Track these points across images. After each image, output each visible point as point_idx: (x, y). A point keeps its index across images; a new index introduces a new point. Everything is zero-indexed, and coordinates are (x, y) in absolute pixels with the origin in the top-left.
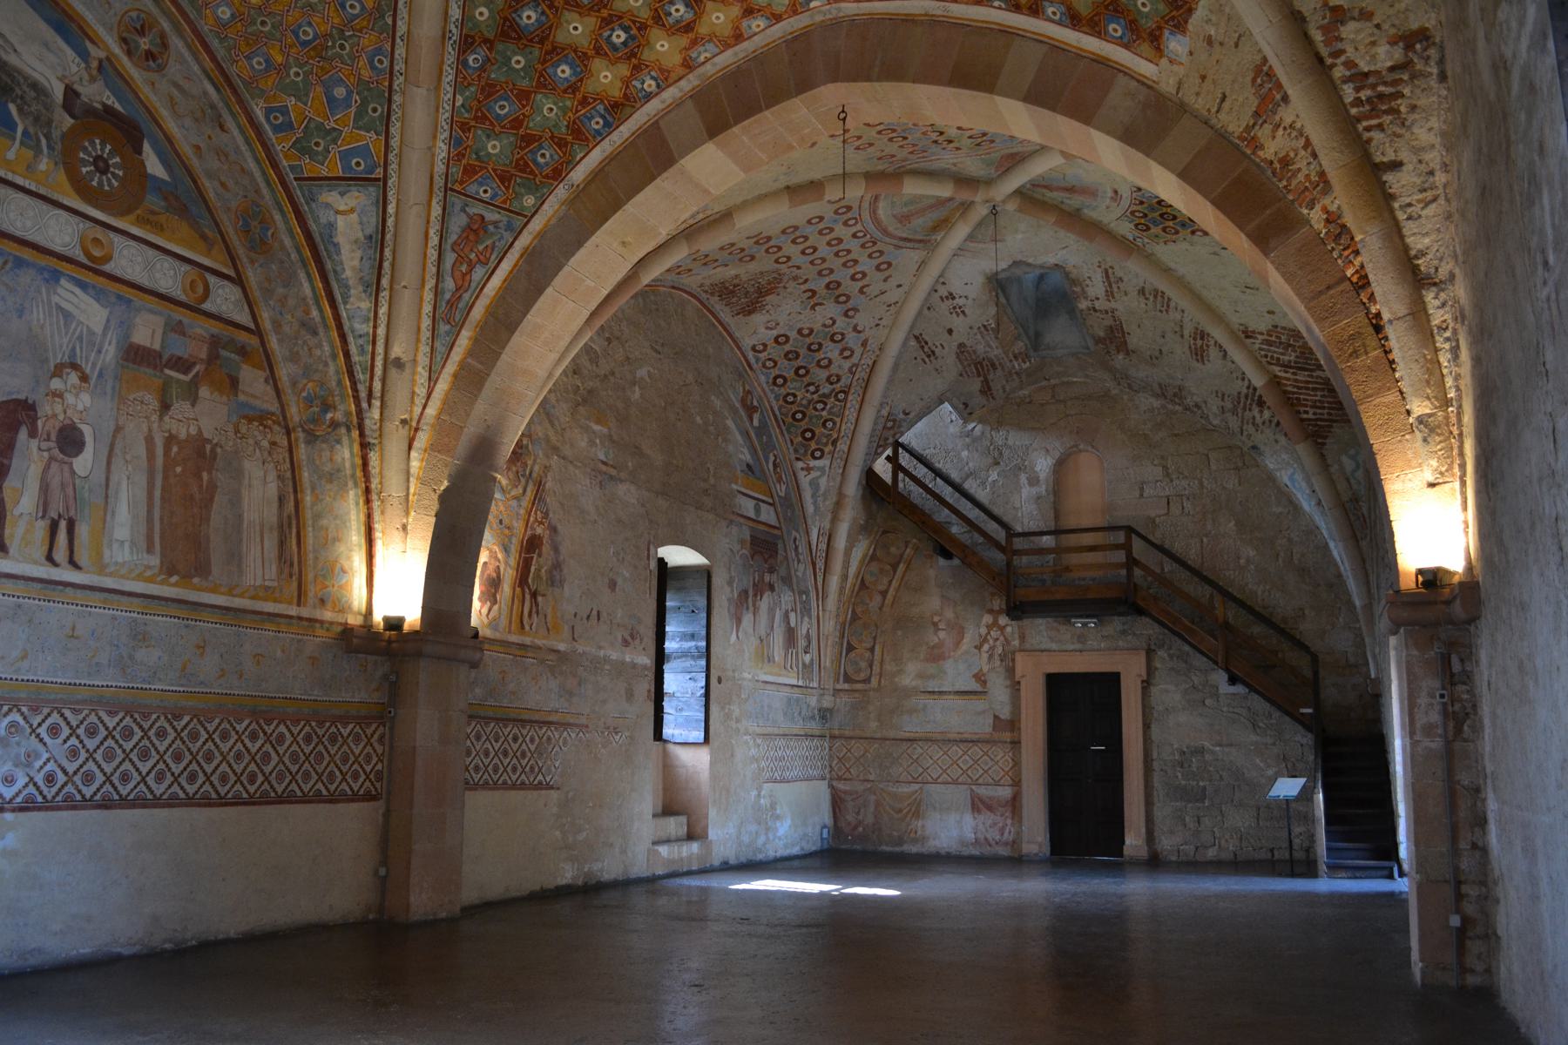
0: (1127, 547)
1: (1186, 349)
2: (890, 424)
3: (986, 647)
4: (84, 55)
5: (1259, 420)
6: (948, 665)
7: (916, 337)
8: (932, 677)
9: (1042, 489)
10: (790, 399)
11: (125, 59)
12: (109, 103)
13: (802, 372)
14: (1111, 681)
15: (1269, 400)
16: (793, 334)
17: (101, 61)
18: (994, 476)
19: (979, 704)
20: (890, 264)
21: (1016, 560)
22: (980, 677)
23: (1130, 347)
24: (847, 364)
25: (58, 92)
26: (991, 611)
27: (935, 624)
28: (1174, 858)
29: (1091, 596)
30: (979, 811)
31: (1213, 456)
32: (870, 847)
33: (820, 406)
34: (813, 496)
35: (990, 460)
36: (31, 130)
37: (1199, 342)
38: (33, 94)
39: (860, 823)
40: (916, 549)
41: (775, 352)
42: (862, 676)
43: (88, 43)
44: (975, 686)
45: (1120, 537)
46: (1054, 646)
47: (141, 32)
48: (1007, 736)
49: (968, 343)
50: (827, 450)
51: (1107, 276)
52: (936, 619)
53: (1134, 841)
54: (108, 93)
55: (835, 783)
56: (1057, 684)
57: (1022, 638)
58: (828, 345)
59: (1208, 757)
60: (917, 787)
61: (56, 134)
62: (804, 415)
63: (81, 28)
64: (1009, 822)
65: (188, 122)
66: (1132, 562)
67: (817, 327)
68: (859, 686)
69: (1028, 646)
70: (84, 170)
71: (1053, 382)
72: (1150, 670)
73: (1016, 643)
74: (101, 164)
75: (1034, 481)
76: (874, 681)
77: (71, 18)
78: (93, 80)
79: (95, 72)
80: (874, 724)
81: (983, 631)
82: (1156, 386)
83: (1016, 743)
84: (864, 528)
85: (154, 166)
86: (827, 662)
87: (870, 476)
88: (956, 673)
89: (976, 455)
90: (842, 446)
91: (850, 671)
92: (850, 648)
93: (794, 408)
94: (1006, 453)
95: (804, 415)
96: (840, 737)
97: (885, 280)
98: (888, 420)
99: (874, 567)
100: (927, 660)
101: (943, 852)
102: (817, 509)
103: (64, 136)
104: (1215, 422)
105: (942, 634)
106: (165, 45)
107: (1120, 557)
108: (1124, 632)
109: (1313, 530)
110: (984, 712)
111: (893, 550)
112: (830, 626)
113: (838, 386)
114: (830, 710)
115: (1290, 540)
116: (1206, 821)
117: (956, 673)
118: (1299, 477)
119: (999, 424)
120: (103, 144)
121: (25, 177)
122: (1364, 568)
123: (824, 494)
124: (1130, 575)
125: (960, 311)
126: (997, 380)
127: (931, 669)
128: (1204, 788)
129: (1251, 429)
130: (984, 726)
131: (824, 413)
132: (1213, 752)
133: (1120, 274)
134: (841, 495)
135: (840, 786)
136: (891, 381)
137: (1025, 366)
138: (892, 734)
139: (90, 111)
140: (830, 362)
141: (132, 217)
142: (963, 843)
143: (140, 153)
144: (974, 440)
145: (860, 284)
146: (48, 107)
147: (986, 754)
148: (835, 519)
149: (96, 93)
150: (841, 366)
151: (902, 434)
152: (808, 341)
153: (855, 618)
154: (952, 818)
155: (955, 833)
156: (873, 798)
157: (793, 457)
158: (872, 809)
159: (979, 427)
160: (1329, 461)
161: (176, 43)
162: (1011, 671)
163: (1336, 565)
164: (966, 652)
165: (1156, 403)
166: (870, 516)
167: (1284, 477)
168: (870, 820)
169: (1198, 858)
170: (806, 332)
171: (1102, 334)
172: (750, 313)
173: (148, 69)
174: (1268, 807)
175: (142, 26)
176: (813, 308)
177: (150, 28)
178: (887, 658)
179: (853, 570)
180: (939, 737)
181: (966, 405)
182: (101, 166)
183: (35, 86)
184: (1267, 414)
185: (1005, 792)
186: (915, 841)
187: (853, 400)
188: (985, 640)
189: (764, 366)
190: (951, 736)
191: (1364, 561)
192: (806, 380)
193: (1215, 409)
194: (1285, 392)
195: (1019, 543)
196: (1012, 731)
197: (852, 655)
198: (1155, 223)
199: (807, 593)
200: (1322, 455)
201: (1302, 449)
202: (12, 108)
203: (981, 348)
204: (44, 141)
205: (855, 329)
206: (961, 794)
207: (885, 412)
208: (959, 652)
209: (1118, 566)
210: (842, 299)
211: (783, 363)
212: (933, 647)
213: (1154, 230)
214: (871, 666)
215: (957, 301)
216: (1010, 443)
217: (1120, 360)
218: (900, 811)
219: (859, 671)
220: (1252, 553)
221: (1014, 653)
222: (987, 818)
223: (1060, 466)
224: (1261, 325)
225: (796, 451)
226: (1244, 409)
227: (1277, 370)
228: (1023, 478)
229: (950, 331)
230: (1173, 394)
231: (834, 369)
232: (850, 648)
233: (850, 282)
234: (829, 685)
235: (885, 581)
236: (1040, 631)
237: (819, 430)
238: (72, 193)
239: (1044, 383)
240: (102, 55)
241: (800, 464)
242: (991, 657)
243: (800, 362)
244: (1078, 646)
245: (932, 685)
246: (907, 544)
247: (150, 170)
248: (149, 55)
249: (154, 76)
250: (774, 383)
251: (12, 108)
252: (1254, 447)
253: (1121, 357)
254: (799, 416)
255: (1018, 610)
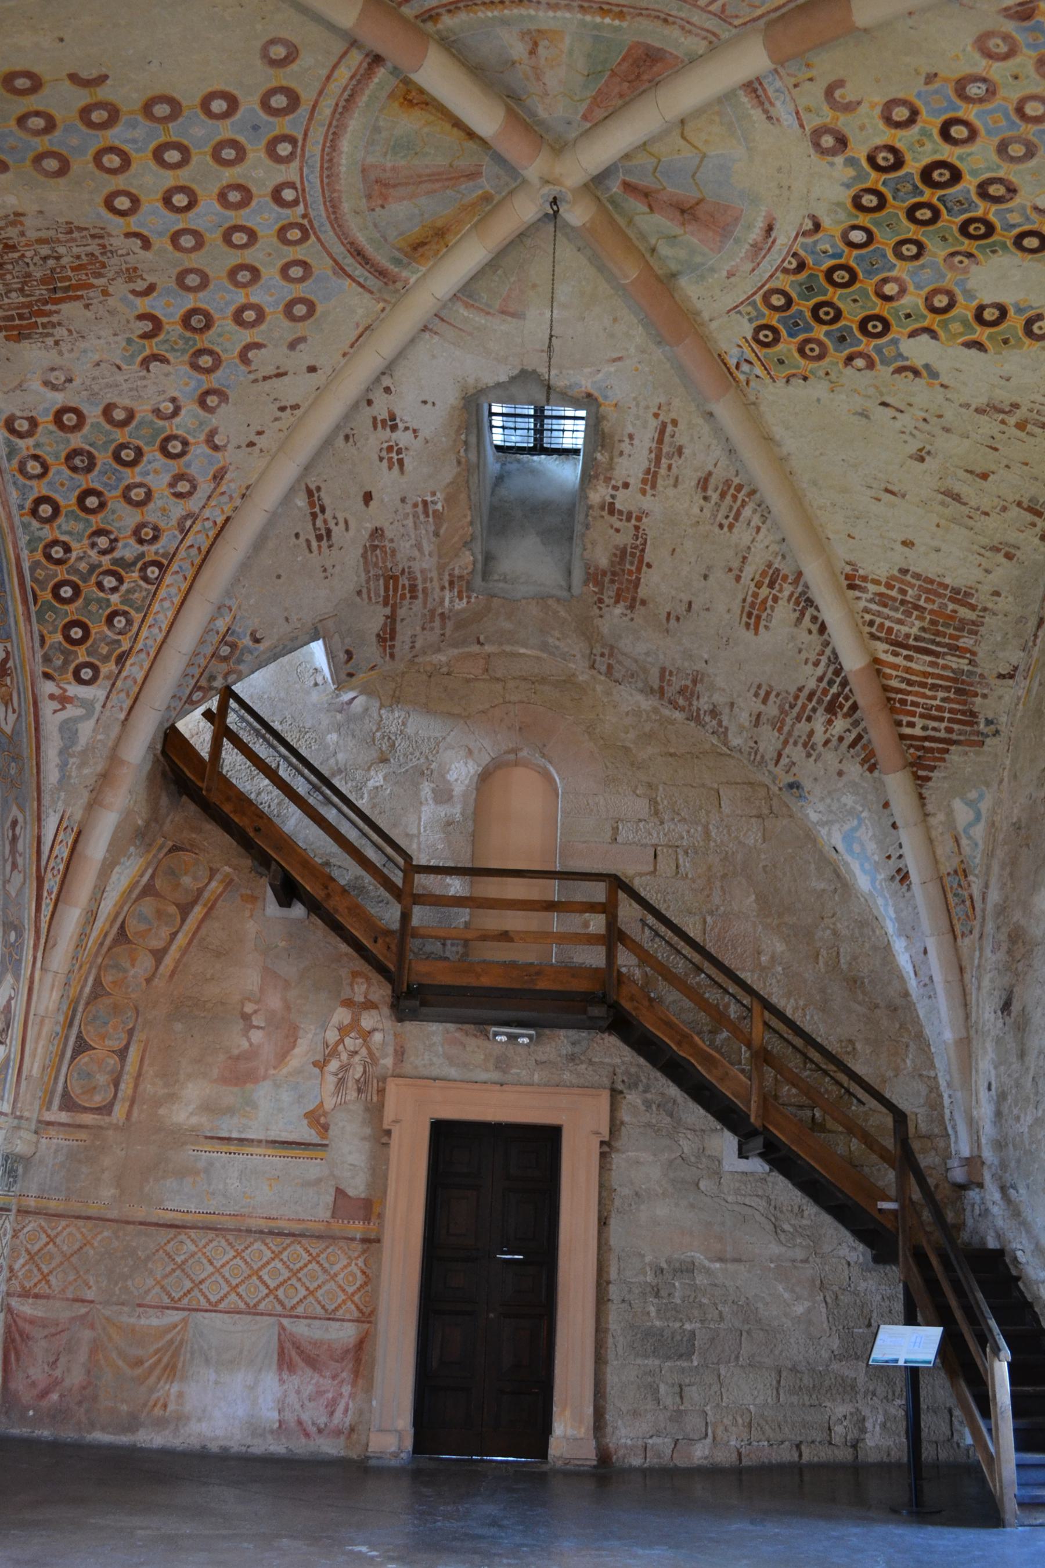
0: (609, 909)
1: (736, 609)
2: (225, 650)
3: (334, 1065)
5: (819, 738)
6: (263, 1093)
7: (310, 493)
8: (230, 1111)
9: (456, 811)
10: (57, 552)
13: (92, 502)
14: (546, 1140)
15: (865, 694)
16: (93, 413)
18: (377, 778)
19: (312, 1168)
20: (311, 307)
21: (419, 915)
22: (317, 1119)
23: (642, 592)
24: (178, 510)
26: (348, 1003)
27: (246, 1017)
28: (636, 1462)
29: (542, 985)
30: (291, 1368)
31: (726, 793)
32: (68, 1434)
33: (109, 582)
34: (64, 752)
35: (374, 754)
37: (764, 591)
39: (56, 1383)
40: (228, 883)
41: (51, 443)
42: (98, 1100)
44: (310, 1135)
45: (598, 892)
46: (453, 1072)
48: (357, 1228)
49: (388, 534)
50: (106, 669)
51: (660, 441)
52: (249, 1008)
53: (569, 1433)
55: (14, 1302)
56: (446, 1136)
57: (400, 1054)
58: (153, 456)
59: (700, 1279)
60: (176, 1316)
62: (77, 590)
64: (346, 1389)
66: (614, 937)
67: (143, 410)
68: (88, 1118)
69: (407, 1068)
71: (488, 648)
72: (615, 1126)
73: (388, 1062)
75: (443, 795)
76: (119, 1111)
80: (108, 1193)
81: (332, 1036)
82: (655, 672)
83: (371, 1242)
84: (139, 835)
86: (34, 1067)
87: (172, 740)
88: (276, 1109)
89: (351, 743)
90: (134, 669)
91: (75, 1090)
92: (82, 1047)
93: (61, 573)
94: (401, 745)
95: (77, 590)
96: (37, 1213)
97: (292, 346)
98: (223, 641)
99: (148, 906)
100: (224, 1080)
101: (214, 1447)
102: (64, 778)
104: (735, 741)
105: (256, 1036)
107: (597, 924)
108: (572, 1058)
109: (868, 923)
110: (318, 1181)
111: (186, 880)
112: (49, 1000)
113: (151, 551)
114: (26, 1160)
115: (835, 933)
116: (693, 1393)
117: (276, 1109)
118: (866, 835)
119: (396, 699)
122: (962, 980)
123: (84, 752)
124: (611, 957)
125: (394, 458)
126: (411, 612)
127: (229, 1095)
128: (693, 1333)
129: (796, 753)
130: (316, 1208)
131: (115, 598)
132: (708, 1272)
133: (682, 439)
134: (114, 759)
135: (26, 1308)
136: (245, 567)
137: (460, 605)
138: (141, 1213)
140: (149, 495)
142: (255, 1429)
144: (351, 719)
145: (247, 336)
147: (314, 1259)
148: (94, 804)
150: (164, 511)
151: (240, 679)
152: (119, 436)
153: (98, 991)
154: (238, 1381)
155: (241, 1411)
156: (87, 1334)
157: (40, 669)
158: (82, 1356)
159: (361, 700)
160: (930, 808)
162: (375, 1111)
163: (901, 979)
164: (299, 1072)
165: (646, 703)
166: (155, 817)
167: (834, 837)
168: (76, 1378)
169: (681, 1462)
170: (119, 415)
171: (604, 562)
172: (20, 337)
174: (794, 1370)
176: (146, 363)
178: (149, 1071)
179: (107, 906)
180: (231, 1224)
181: (349, 654)
184: (840, 724)
185: (345, 1333)
186: (161, 1423)
187: (173, 584)
188: (334, 1053)
189: (22, 470)
190: (254, 1223)
191: (961, 969)
192: (96, 521)
193: (744, 718)
194: (886, 689)
195: (425, 883)
196: (367, 1219)
197: (84, 1059)
198: (794, 329)
199: (19, 930)
200: (921, 797)
201: (897, 784)
203: (405, 547)
205: (210, 440)
206: (262, 1334)
207: (221, 625)
208: (285, 1071)
209: (592, 939)
210: (206, 361)
211: (59, 471)
212: (238, 1058)
213: (787, 346)
214: (116, 1084)
215: (402, 438)
216: (410, 731)
217: (614, 617)
218: (139, 1362)
219: (93, 1090)
220: (780, 947)
221: (383, 1079)
222: (305, 1381)
223: (485, 777)
224: (879, 566)
225: (47, 659)
226: (798, 719)
227: (881, 649)
228: (426, 789)
229: (368, 497)
230: (678, 692)
231: (151, 514)
232: (82, 1047)
233: (230, 325)
234: (31, 1111)
235: (165, 932)
236: (433, 1042)
237: (98, 628)
239: (475, 648)
241: (49, 687)
242: (341, 1082)
243: (93, 480)
244: (495, 1076)
245: (228, 1127)
246: (213, 872)
250: (34, 512)
252: (794, 786)
253: (618, 610)
254: (66, 592)
255: (411, 1000)
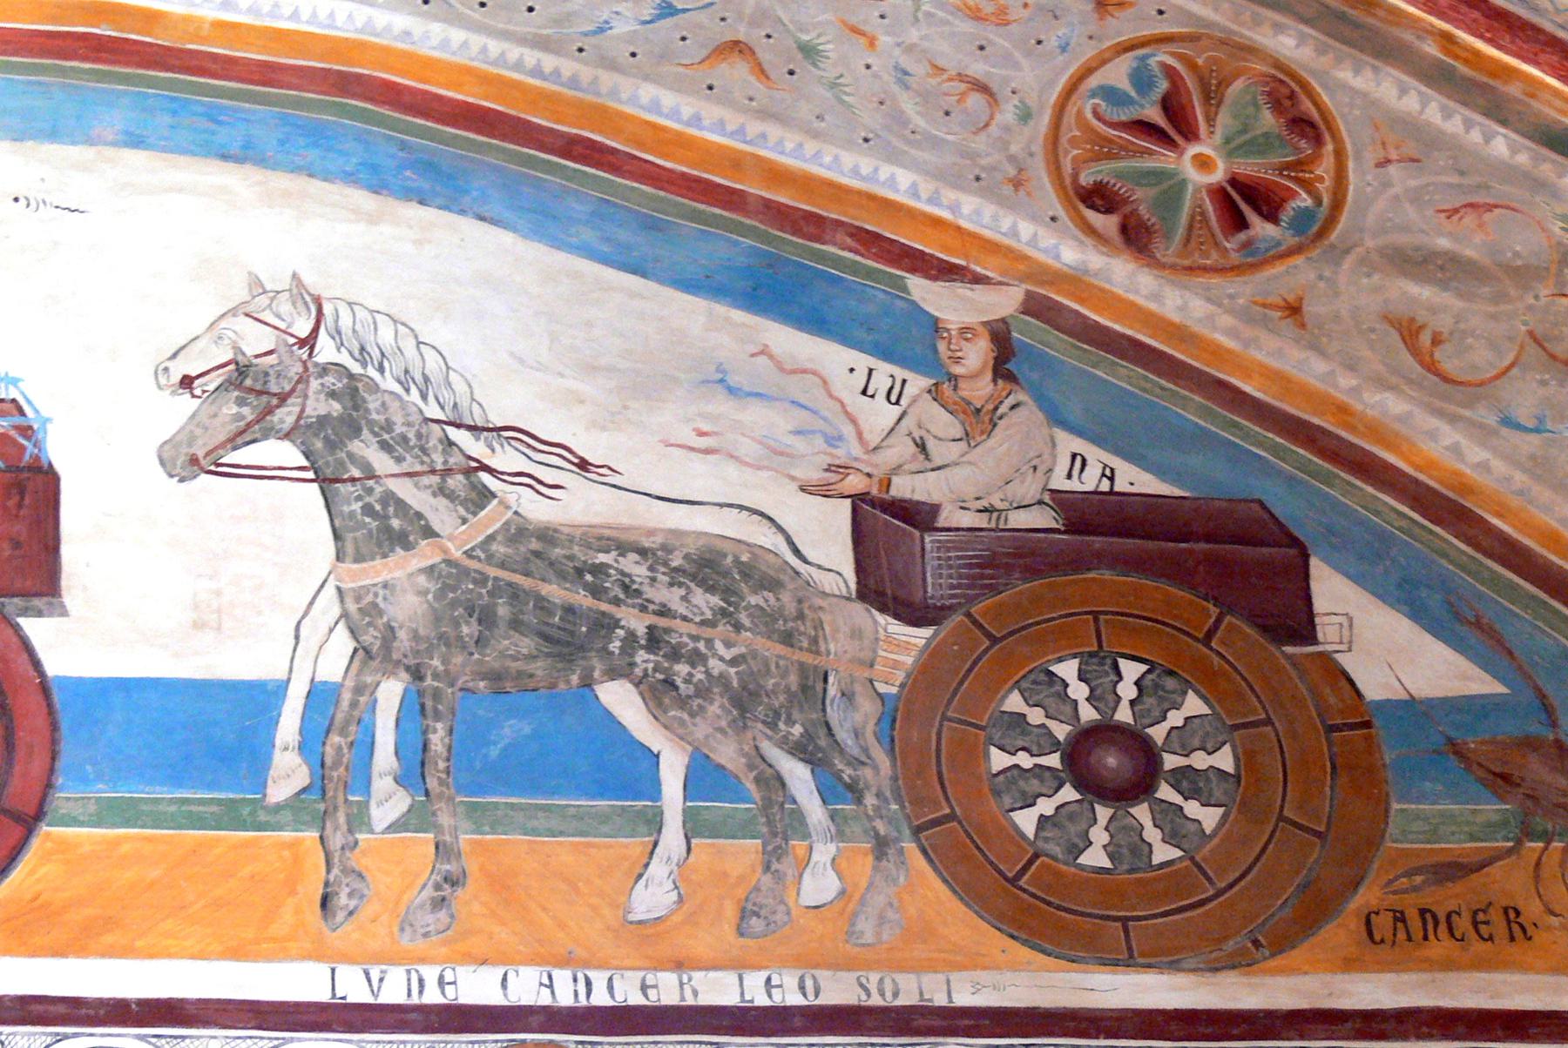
4: (913, 343)
11: (1122, 275)
12: (1090, 480)
17: (1001, 337)
25: (826, 541)
36: (727, 753)
38: (706, 602)
43: (920, 288)
47: (1175, 123)
54: (1069, 443)
61: (856, 722)
63: (869, 241)
65: (1527, 395)
70: (1026, 821)
74: (1111, 761)
77: (812, 226)
78: (980, 422)
79: (981, 389)
85: (1387, 651)
103: (898, 718)
106: (1305, 123)
120: (1101, 669)
121: (740, 965)
139: (1005, 559)
141: (1340, 931)
143: (1302, 626)
146: (795, 626)
149: (1004, 473)
161: (1359, 89)
173: (1255, 260)
175: (1173, 106)
177: (1212, 96)
182: (1112, 766)
183: (708, 567)
202: (620, 700)
204: (798, 775)
238: (995, 941)
240: (1003, 302)
247: (1375, 684)
248: (1244, 201)
249: (1294, 276)
251: (620, 700)
